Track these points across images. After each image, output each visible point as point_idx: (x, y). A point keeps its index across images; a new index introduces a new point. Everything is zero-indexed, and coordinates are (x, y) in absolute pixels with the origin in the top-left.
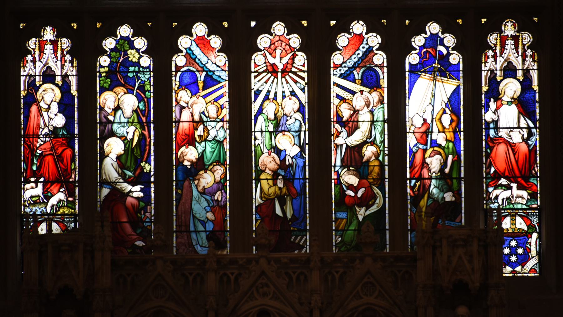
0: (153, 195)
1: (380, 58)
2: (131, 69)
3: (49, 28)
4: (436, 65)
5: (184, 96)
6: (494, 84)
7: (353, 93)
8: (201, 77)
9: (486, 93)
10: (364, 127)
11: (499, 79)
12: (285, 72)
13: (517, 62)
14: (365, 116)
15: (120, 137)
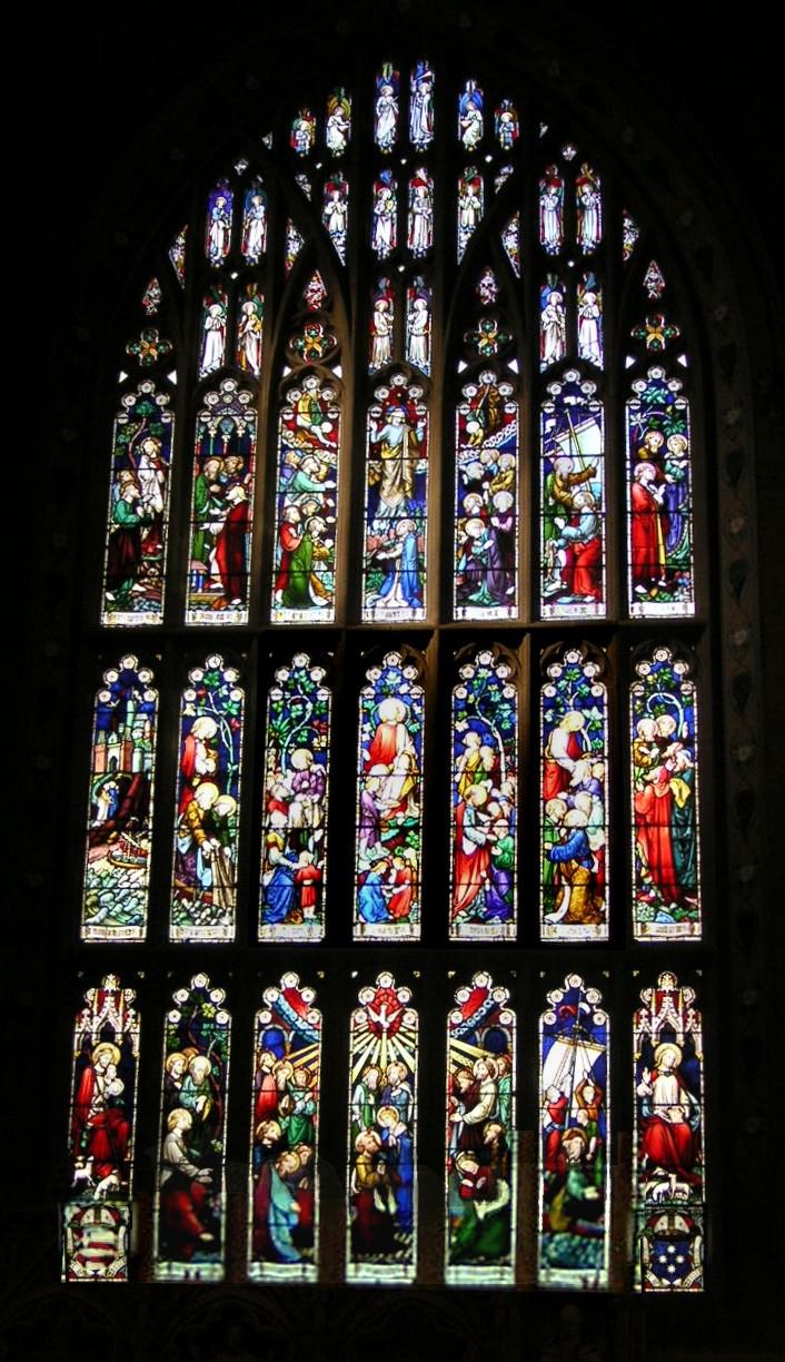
0: (223, 1179)
1: (508, 1017)
2: (205, 1026)
3: (111, 977)
4: (577, 1025)
5: (268, 1059)
6: (648, 1050)
7: (474, 1059)
8: (289, 1037)
9: (639, 1061)
10: (487, 1101)
11: (654, 1043)
12: (392, 1031)
13: (677, 1023)
14: (488, 1088)
15: (188, 1109)
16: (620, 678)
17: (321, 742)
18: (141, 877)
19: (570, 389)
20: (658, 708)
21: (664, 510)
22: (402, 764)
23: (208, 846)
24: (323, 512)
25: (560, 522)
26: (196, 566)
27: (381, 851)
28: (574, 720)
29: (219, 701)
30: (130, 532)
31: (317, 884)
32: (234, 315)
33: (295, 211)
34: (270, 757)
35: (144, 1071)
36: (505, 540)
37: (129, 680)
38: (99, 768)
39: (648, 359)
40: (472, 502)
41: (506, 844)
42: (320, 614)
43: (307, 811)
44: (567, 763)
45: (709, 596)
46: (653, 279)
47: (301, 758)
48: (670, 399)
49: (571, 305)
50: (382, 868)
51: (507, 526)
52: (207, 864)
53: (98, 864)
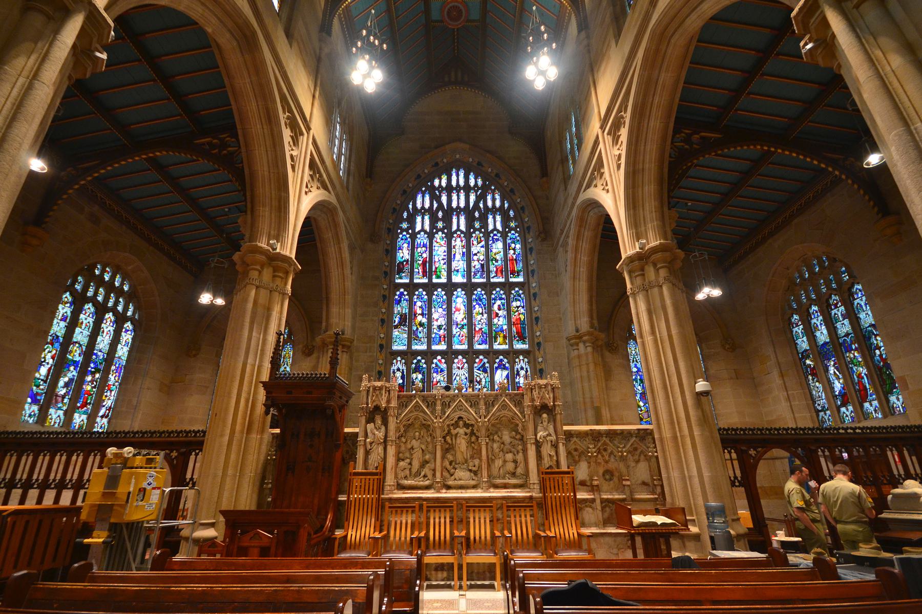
5: (435, 375)
6: (518, 372)
8: (439, 370)
12: (462, 368)
13: (524, 366)
14: (483, 380)
16: (508, 294)
17: (444, 307)
18: (405, 336)
19: (495, 235)
20: (517, 300)
21: (516, 260)
22: (462, 312)
23: (420, 329)
24: (443, 259)
25: (494, 262)
26: (416, 270)
27: (458, 330)
28: (499, 302)
29: (422, 298)
31: (444, 337)
32: (423, 219)
33: (435, 197)
34: (433, 310)
36: (482, 265)
37: (402, 294)
38: (396, 312)
39: (511, 229)
40: (475, 258)
41: (485, 329)
42: (443, 280)
43: (442, 321)
44: (498, 311)
45: (527, 276)
46: (512, 213)
47: (440, 310)
48: (516, 237)
49: (494, 218)
50: (459, 333)
51: (483, 263)
52: (420, 333)
53: (396, 333)
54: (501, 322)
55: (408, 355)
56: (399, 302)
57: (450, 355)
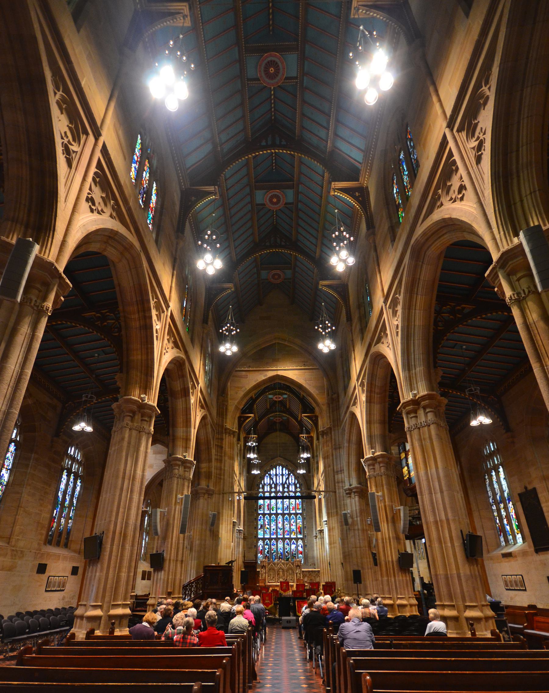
16: (296, 517)
18: (263, 532)
23: (267, 530)
28: (293, 520)
30: (260, 505)
33: (271, 479)
35: (263, 547)
37: (261, 517)
41: (288, 530)
42: (275, 512)
43: (274, 527)
46: (298, 485)
53: (259, 531)
54: (293, 527)
55: (264, 539)
56: (260, 520)
57: (277, 539)
